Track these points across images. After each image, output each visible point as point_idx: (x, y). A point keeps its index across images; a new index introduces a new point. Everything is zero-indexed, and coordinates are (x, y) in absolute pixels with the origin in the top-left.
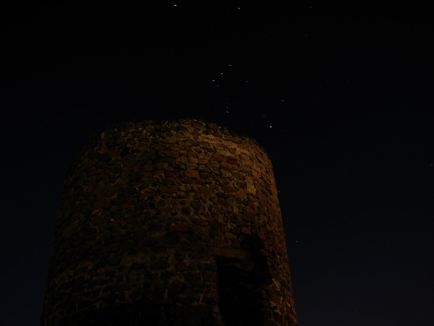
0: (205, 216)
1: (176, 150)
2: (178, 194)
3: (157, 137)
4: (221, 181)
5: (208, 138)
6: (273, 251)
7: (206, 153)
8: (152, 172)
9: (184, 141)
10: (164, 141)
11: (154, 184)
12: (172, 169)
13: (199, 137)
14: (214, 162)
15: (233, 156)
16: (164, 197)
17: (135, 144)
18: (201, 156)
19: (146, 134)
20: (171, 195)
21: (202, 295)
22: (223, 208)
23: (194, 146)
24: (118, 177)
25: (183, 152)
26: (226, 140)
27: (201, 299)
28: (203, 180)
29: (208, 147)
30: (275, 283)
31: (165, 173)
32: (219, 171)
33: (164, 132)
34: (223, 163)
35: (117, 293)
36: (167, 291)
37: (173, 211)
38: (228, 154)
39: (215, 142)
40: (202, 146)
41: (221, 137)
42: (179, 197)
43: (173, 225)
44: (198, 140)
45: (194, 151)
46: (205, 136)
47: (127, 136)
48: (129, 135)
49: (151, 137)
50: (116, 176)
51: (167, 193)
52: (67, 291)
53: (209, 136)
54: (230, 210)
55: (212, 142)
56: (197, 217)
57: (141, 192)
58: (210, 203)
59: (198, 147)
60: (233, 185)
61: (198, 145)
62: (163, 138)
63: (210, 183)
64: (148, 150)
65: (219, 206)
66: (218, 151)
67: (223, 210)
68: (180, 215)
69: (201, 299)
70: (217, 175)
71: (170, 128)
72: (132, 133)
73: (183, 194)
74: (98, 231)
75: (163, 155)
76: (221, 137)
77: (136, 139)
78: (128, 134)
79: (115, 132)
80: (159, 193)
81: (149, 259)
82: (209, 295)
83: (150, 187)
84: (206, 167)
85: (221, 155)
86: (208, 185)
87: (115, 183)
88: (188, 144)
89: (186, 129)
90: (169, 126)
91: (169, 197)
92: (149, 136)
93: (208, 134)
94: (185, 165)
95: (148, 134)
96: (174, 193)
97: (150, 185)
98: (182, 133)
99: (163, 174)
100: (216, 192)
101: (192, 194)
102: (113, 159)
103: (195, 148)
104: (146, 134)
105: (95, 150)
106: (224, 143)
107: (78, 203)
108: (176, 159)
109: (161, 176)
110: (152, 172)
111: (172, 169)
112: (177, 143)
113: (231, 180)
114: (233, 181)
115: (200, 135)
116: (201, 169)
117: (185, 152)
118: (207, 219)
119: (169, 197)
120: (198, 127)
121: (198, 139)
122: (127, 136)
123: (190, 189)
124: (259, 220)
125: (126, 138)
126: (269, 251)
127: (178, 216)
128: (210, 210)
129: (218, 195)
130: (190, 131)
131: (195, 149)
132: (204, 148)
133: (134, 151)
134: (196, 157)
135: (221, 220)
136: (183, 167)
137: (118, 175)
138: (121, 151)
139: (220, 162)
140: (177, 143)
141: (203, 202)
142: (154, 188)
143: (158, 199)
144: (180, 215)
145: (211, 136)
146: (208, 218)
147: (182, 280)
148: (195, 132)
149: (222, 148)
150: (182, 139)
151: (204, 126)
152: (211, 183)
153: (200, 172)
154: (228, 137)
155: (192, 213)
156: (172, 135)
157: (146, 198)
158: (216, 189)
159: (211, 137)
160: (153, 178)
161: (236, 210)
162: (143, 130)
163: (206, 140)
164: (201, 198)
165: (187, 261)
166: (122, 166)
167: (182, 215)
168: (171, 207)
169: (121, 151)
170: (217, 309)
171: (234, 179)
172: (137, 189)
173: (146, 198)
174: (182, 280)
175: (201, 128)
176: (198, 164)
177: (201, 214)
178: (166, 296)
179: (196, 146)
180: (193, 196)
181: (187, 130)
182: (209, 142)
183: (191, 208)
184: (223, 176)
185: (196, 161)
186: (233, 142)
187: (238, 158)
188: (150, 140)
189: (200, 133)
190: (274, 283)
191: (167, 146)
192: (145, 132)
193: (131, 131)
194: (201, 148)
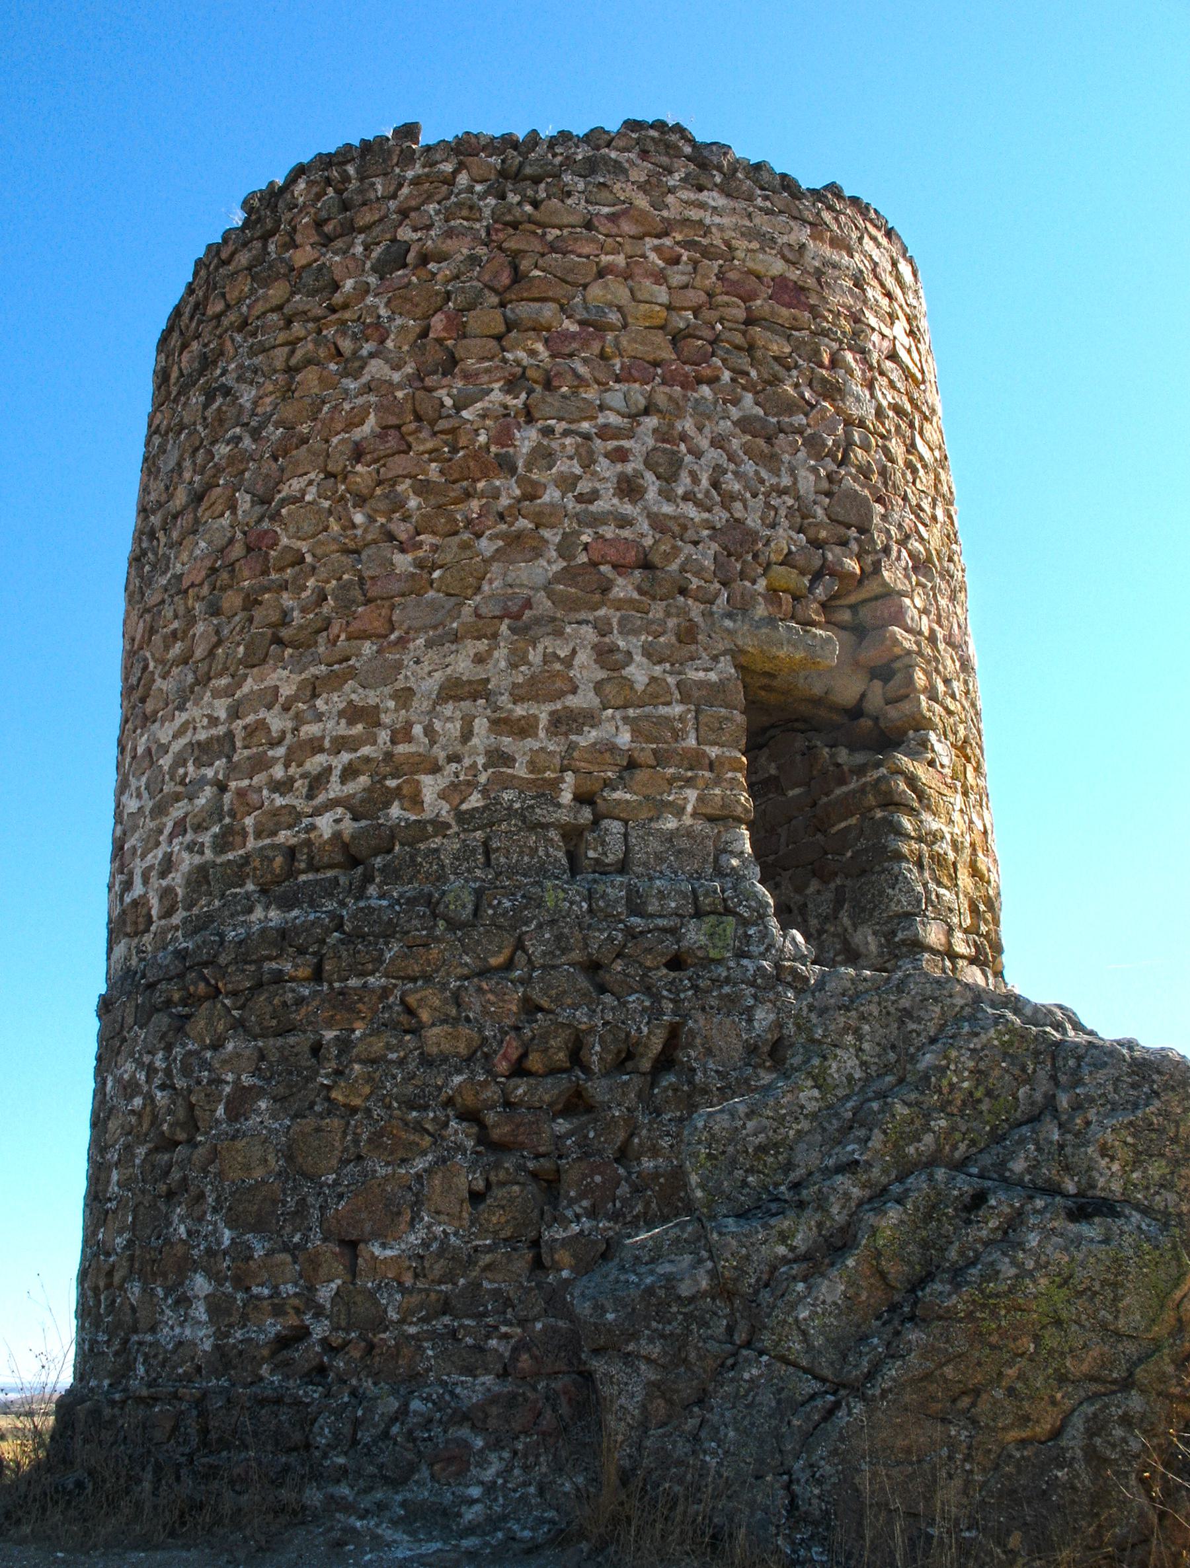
0: (698, 504)
1: (586, 250)
2: (601, 420)
3: (513, 198)
4: (753, 373)
5: (702, 206)
6: (932, 631)
7: (695, 264)
8: (499, 338)
9: (613, 218)
10: (538, 216)
11: (511, 386)
12: (574, 328)
13: (670, 199)
14: (726, 298)
15: (794, 274)
16: (548, 432)
17: (429, 227)
18: (677, 277)
19: (470, 190)
20: (573, 427)
21: (692, 795)
22: (764, 474)
23: (650, 235)
24: (372, 355)
25: (610, 258)
26: (768, 212)
27: (689, 808)
28: (687, 368)
29: (705, 241)
30: (938, 747)
31: (546, 342)
32: (744, 333)
33: (536, 180)
34: (759, 302)
35: (392, 783)
36: (569, 777)
37: (584, 487)
38: (778, 267)
39: (726, 221)
40: (679, 237)
41: (750, 198)
42: (605, 432)
43: (585, 538)
44: (665, 213)
45: (653, 256)
46: (691, 195)
47: (394, 196)
48: (405, 190)
49: (491, 201)
50: (364, 352)
51: (560, 419)
52: (209, 773)
53: (704, 196)
54: (786, 481)
55: (717, 220)
56: (667, 509)
57: (464, 413)
58: (714, 455)
59: (668, 241)
60: (796, 386)
61: (667, 234)
62: (536, 204)
63: (713, 381)
64: (481, 251)
65: (749, 467)
66: (740, 254)
67: (762, 482)
69: (689, 808)
70: (738, 348)
71: (561, 165)
72: (416, 182)
73: (613, 419)
74: (309, 558)
75: (537, 273)
76: (750, 198)
77: (431, 208)
78: (400, 186)
79: (346, 178)
80: (530, 419)
81: (503, 664)
82: (717, 791)
83: (497, 396)
84: (696, 317)
85: (751, 272)
86: (705, 390)
87: (365, 378)
88: (627, 227)
89: (618, 169)
90: (555, 155)
91: (566, 433)
92: (482, 197)
93: (700, 189)
94: (620, 309)
95: (479, 188)
96: (585, 419)
97: (497, 386)
98: (604, 185)
99: (540, 347)
100: (735, 413)
101: (651, 422)
102: (349, 284)
103: (656, 242)
104: (470, 190)
105: (272, 248)
106: (760, 220)
107: (222, 450)
108: (585, 286)
109: (533, 353)
110: (499, 338)
111: (574, 328)
112: (589, 226)
113: (789, 369)
114: (795, 373)
115: (671, 190)
116: (682, 325)
117: (620, 260)
118: (706, 515)
119: (566, 433)
120: (665, 160)
121: (667, 207)
122: (394, 196)
123: (642, 402)
124: (884, 517)
125: (392, 204)
126: (920, 633)
128: (715, 484)
129: (744, 424)
130: (634, 175)
131: (657, 249)
132: (688, 244)
133: (424, 259)
134: (660, 277)
135: (753, 521)
136: (614, 317)
137: (368, 347)
138: (374, 255)
139: (747, 298)
140: (589, 226)
141: (690, 451)
142: (509, 397)
143: (527, 439)
145: (715, 194)
146: (709, 511)
147: (624, 738)
148: (654, 180)
149: (755, 245)
150: (606, 210)
151: (689, 158)
152: (717, 379)
153: (677, 338)
154: (775, 198)
155: (652, 494)
156: (569, 194)
157: (482, 439)
158: (736, 402)
159: (714, 198)
160: (505, 361)
161: (807, 483)
162: (456, 172)
163: (694, 214)
164: (683, 437)
165: (639, 673)
166: (383, 312)
167: (615, 501)
168: (578, 470)
169: (374, 255)
171: (797, 366)
172: (448, 402)
173: (482, 439)
174: (624, 738)
175: (679, 163)
176: (669, 308)
177: (686, 497)
179: (658, 236)
180: (655, 431)
181: (625, 172)
182: (708, 221)
183: (649, 476)
184: (759, 354)
185: (662, 294)
186: (795, 218)
187: (811, 282)
188: (487, 212)
189: (671, 183)
190: (933, 751)
191: (549, 238)
192: (463, 179)
193: (410, 174)
194: (678, 243)
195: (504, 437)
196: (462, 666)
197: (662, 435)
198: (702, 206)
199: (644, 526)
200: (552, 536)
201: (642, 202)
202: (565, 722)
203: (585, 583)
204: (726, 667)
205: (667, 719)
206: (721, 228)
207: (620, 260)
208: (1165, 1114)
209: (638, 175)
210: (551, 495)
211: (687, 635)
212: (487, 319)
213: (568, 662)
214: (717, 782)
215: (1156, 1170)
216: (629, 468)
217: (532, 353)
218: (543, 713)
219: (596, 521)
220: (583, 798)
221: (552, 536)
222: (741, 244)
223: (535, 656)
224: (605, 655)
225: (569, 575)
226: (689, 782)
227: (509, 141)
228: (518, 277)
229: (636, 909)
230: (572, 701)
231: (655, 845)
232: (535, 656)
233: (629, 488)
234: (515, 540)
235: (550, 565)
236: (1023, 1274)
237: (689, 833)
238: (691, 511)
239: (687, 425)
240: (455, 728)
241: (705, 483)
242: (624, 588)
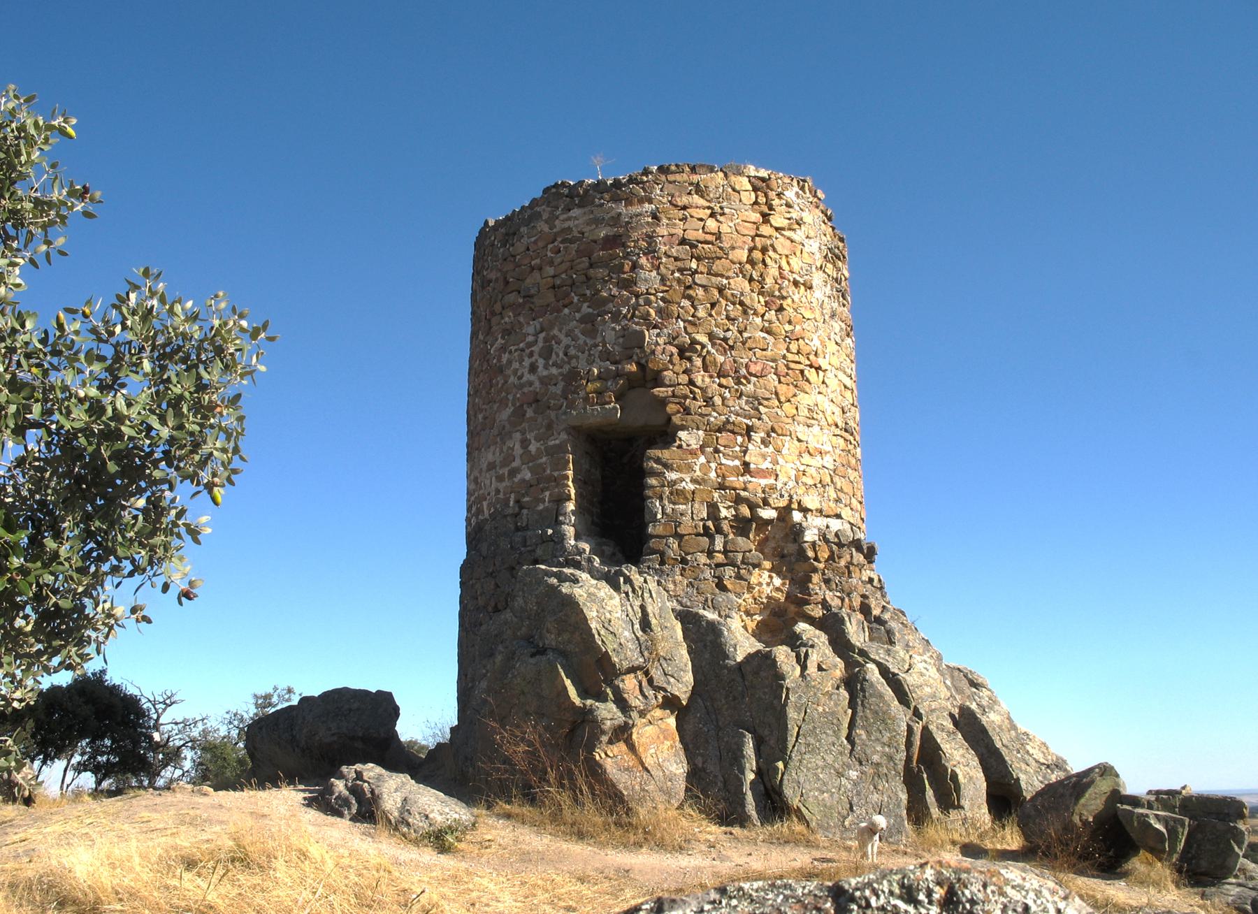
9: (535, 242)
16: (510, 352)
21: (547, 493)
36: (513, 496)
46: (565, 216)
53: (572, 213)
56: (545, 373)
58: (566, 341)
68: (528, 377)
83: (500, 341)
89: (539, 215)
100: (578, 316)
101: (542, 335)
127: (525, 379)
134: (551, 263)
144: (528, 377)
163: (566, 225)
165: (533, 448)
170: (571, 506)
174: (528, 476)
178: (512, 503)
185: (550, 271)
195: (499, 360)
196: (490, 457)
197: (546, 340)
198: (569, 219)
199: (537, 384)
200: (510, 397)
201: (546, 229)
202: (513, 473)
203: (519, 413)
204: (564, 436)
205: (541, 464)
206: (576, 226)
207: (538, 261)
208: (566, 615)
209: (545, 216)
210: (512, 379)
211: (549, 427)
212: (498, 307)
213: (512, 449)
214: (557, 486)
215: (566, 636)
216: (533, 359)
217: (509, 317)
218: (505, 471)
219: (522, 386)
220: (517, 502)
221: (510, 397)
222: (587, 229)
223: (505, 449)
224: (525, 443)
225: (514, 413)
226: (547, 489)
227: (508, 218)
228: (507, 283)
229: (525, 546)
230: (514, 464)
231: (536, 517)
232: (505, 449)
233: (533, 368)
234: (501, 401)
235: (509, 410)
236: (514, 677)
237: (546, 509)
238: (554, 371)
239: (555, 332)
240: (488, 482)
241: (561, 355)
242: (530, 413)
